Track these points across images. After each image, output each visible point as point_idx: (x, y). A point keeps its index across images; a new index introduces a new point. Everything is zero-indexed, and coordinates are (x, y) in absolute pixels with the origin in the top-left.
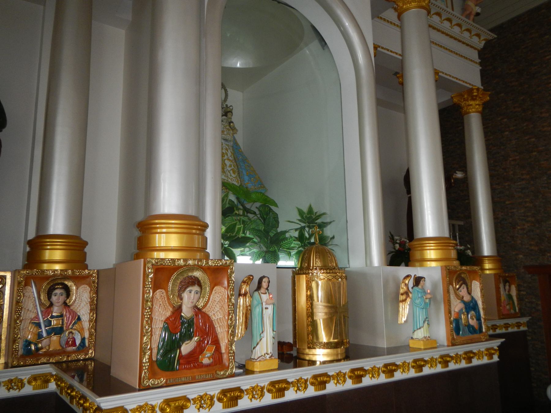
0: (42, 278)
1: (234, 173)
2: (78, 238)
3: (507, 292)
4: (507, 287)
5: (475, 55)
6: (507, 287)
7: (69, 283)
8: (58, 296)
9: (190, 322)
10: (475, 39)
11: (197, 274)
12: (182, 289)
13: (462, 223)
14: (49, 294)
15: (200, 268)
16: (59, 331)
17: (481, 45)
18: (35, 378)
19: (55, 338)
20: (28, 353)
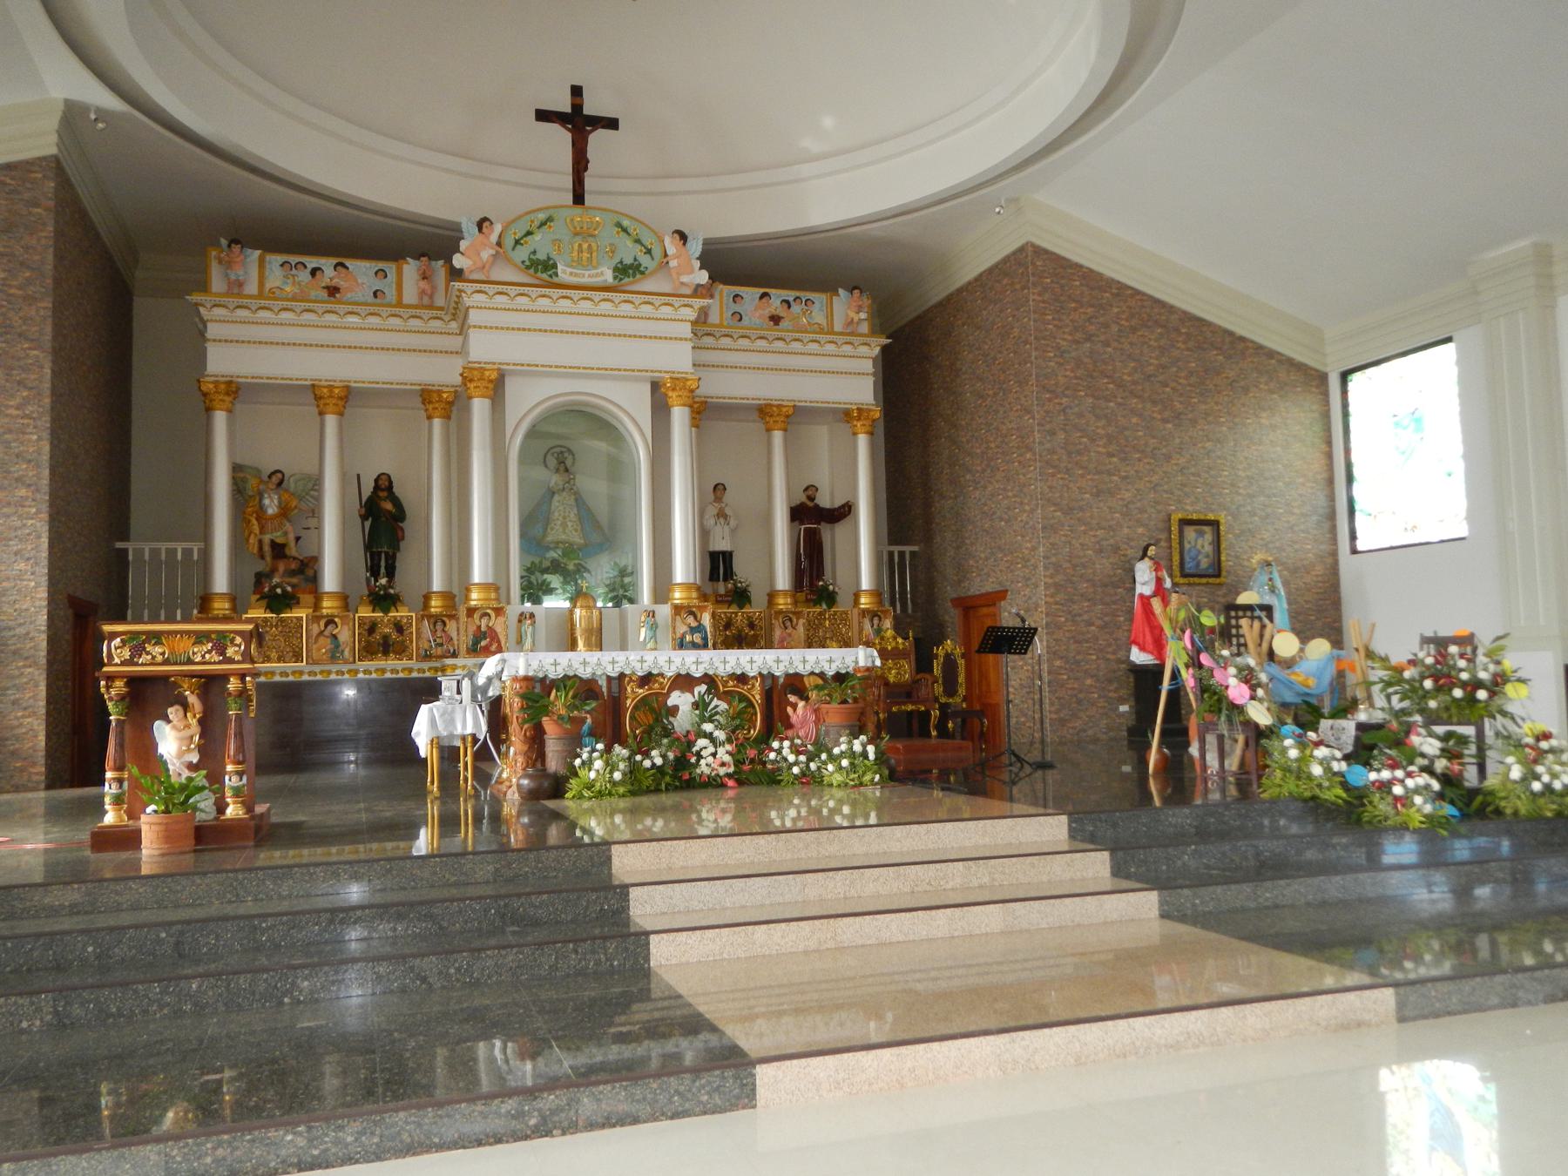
0: (430, 616)
1: (576, 530)
2: (451, 593)
3: (875, 627)
4: (876, 621)
5: (868, 366)
6: (876, 621)
7: (445, 619)
8: (439, 626)
9: (485, 633)
10: (864, 350)
11: (489, 611)
12: (481, 618)
13: (916, 548)
14: (435, 624)
15: (489, 608)
16: (442, 645)
17: (877, 350)
18: (430, 669)
19: (439, 649)
20: (426, 655)
